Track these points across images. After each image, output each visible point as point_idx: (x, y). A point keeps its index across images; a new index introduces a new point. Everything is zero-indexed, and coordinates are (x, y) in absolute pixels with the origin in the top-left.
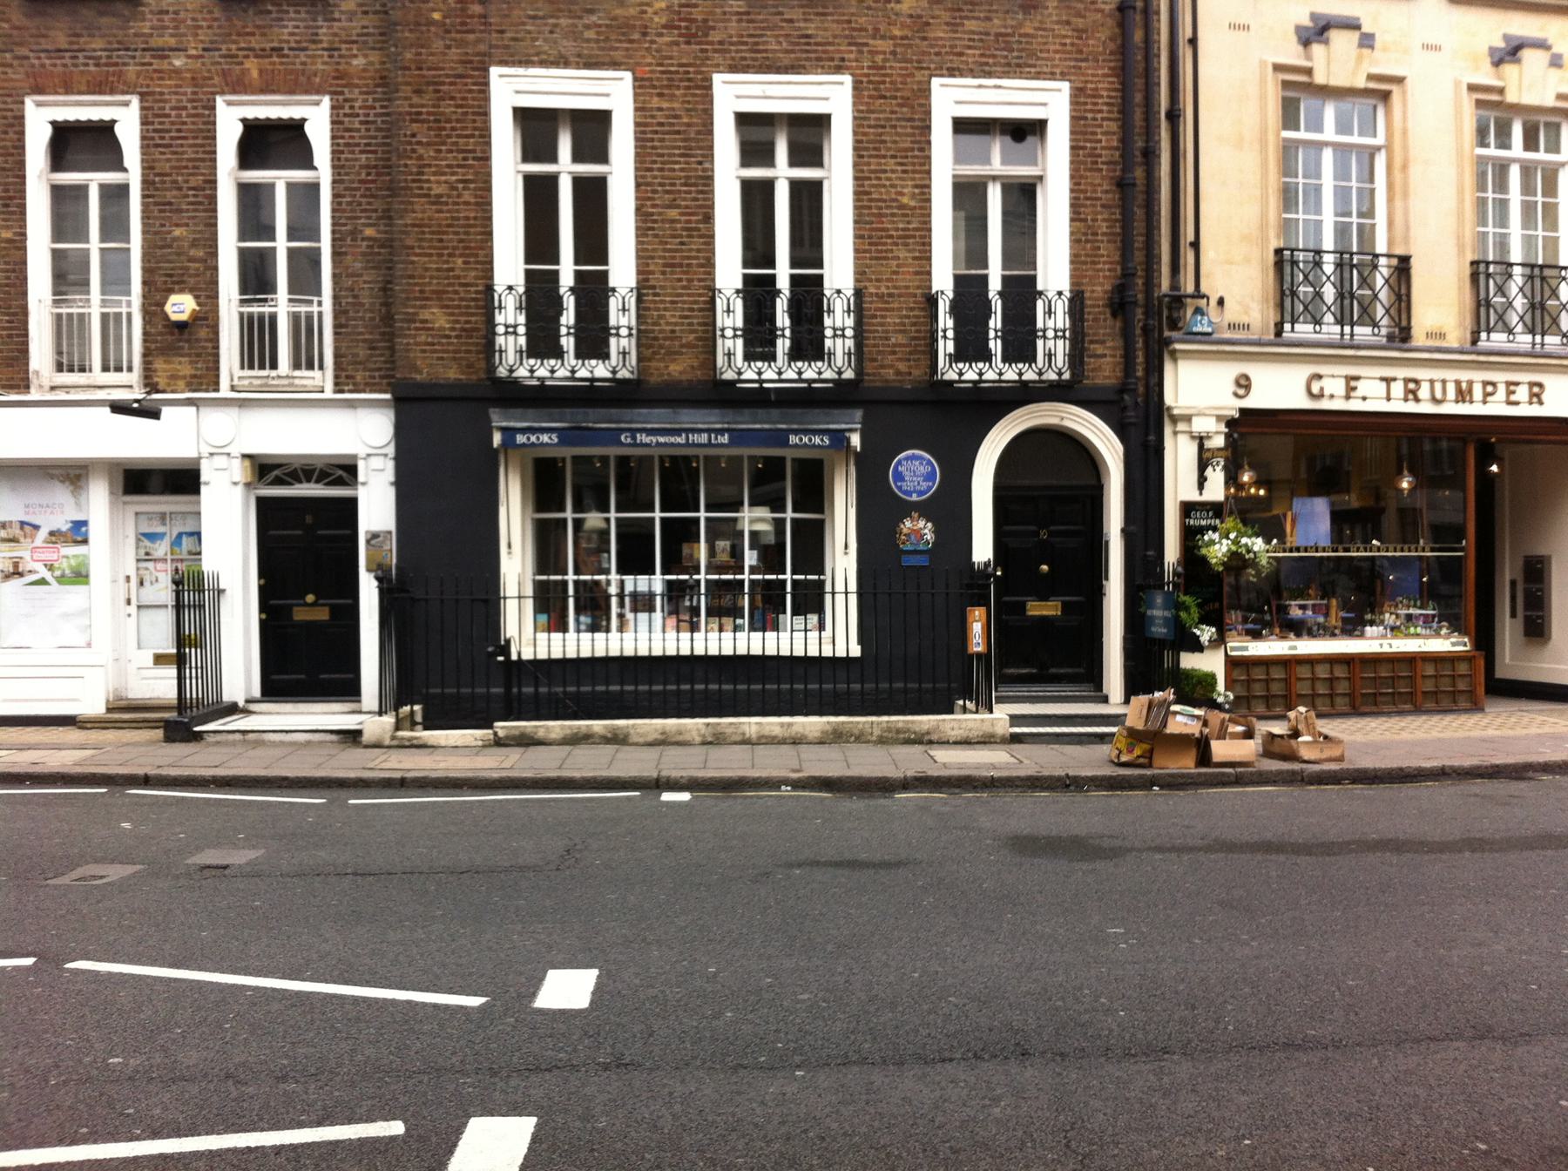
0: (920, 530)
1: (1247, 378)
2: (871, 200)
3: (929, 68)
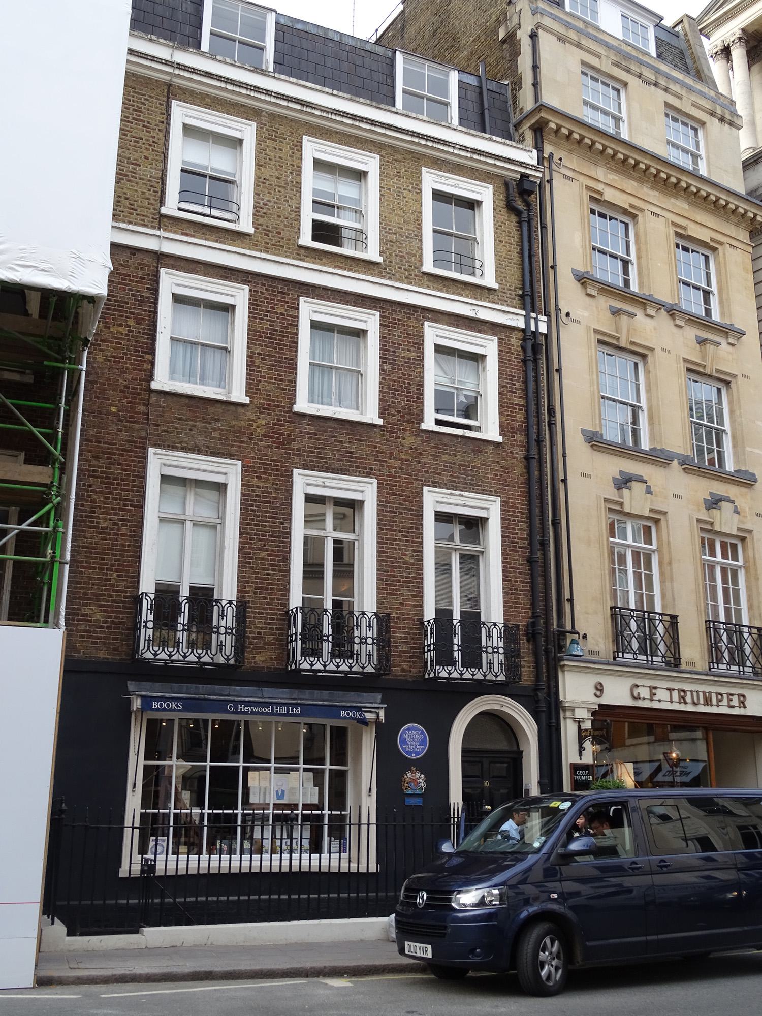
0: (416, 780)
1: (601, 685)
2: (387, 557)
3: (422, 480)
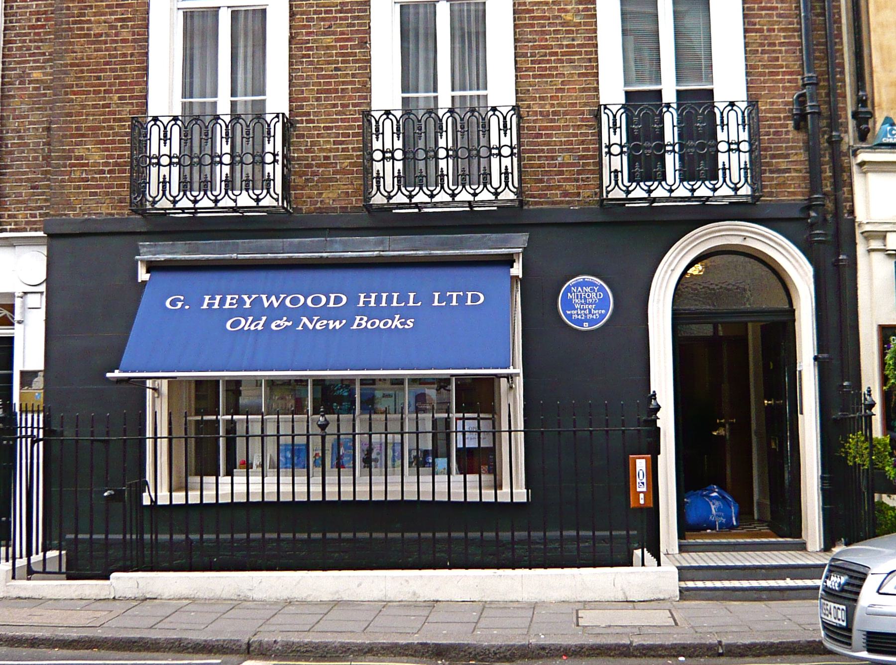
2: (533, 18)
